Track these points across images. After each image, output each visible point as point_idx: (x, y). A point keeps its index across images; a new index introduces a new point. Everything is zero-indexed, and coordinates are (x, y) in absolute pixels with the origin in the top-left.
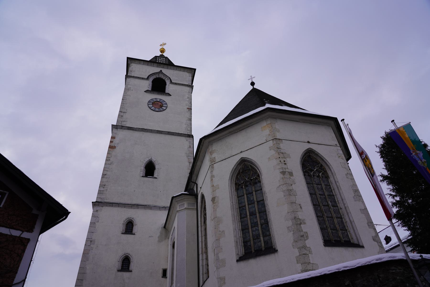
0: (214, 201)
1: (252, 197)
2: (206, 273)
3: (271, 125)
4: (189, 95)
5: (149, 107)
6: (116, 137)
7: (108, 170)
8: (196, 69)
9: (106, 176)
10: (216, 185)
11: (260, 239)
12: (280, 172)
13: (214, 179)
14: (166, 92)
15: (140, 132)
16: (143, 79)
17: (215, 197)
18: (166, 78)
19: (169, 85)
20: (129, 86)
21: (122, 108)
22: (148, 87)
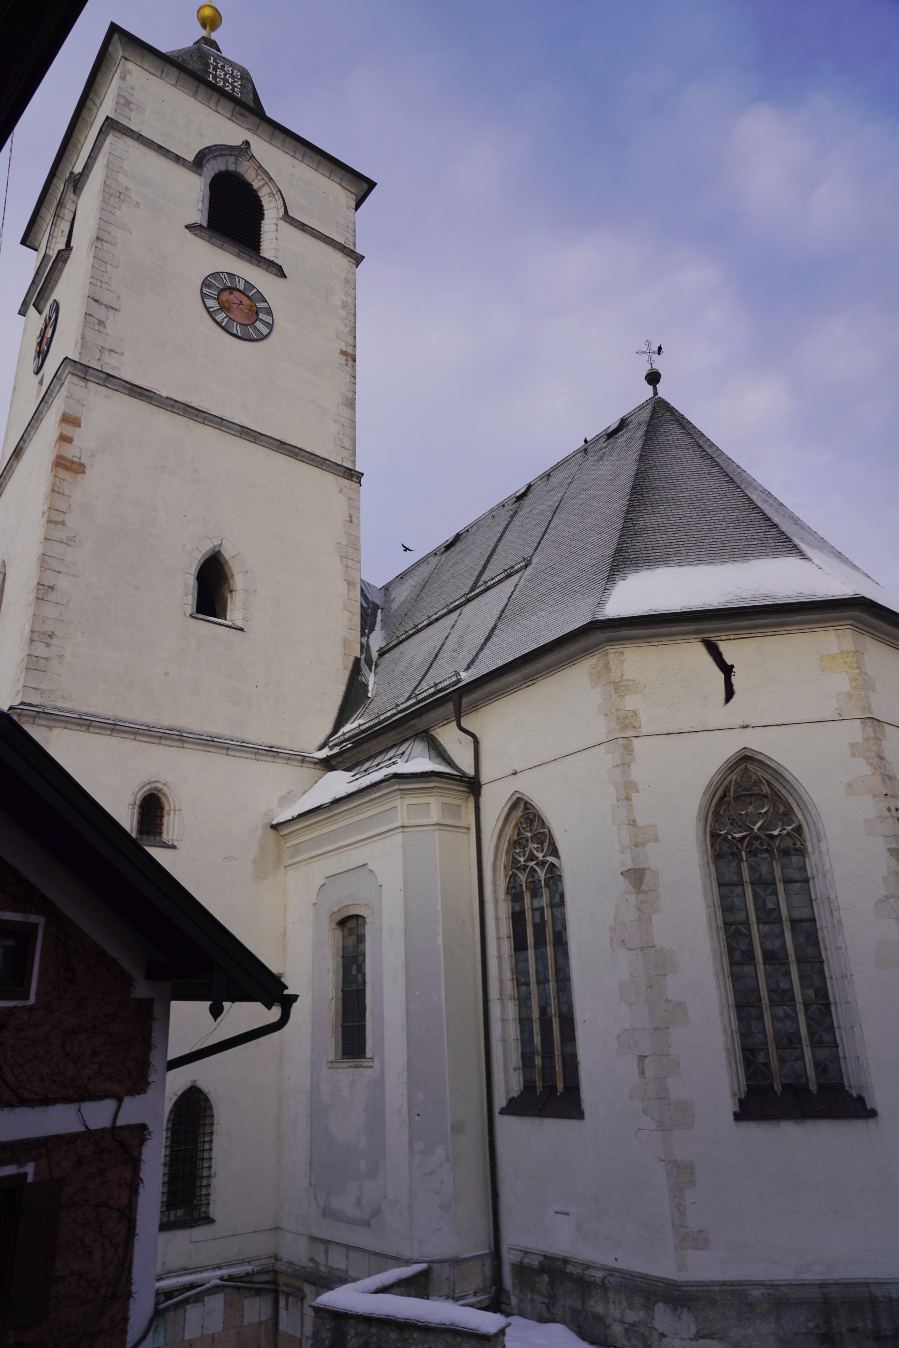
0: (641, 882)
1: (770, 897)
2: (519, 1068)
3: (855, 659)
4: (347, 294)
5: (207, 308)
6: (83, 418)
7: (62, 569)
8: (376, 184)
9: (52, 596)
10: (648, 826)
11: (799, 1050)
12: (889, 850)
13: (634, 796)
14: (261, 255)
15: (176, 415)
16: (178, 162)
17: (645, 869)
18: (266, 186)
19: (277, 225)
20: (120, 175)
21: (99, 283)
22: (199, 210)
